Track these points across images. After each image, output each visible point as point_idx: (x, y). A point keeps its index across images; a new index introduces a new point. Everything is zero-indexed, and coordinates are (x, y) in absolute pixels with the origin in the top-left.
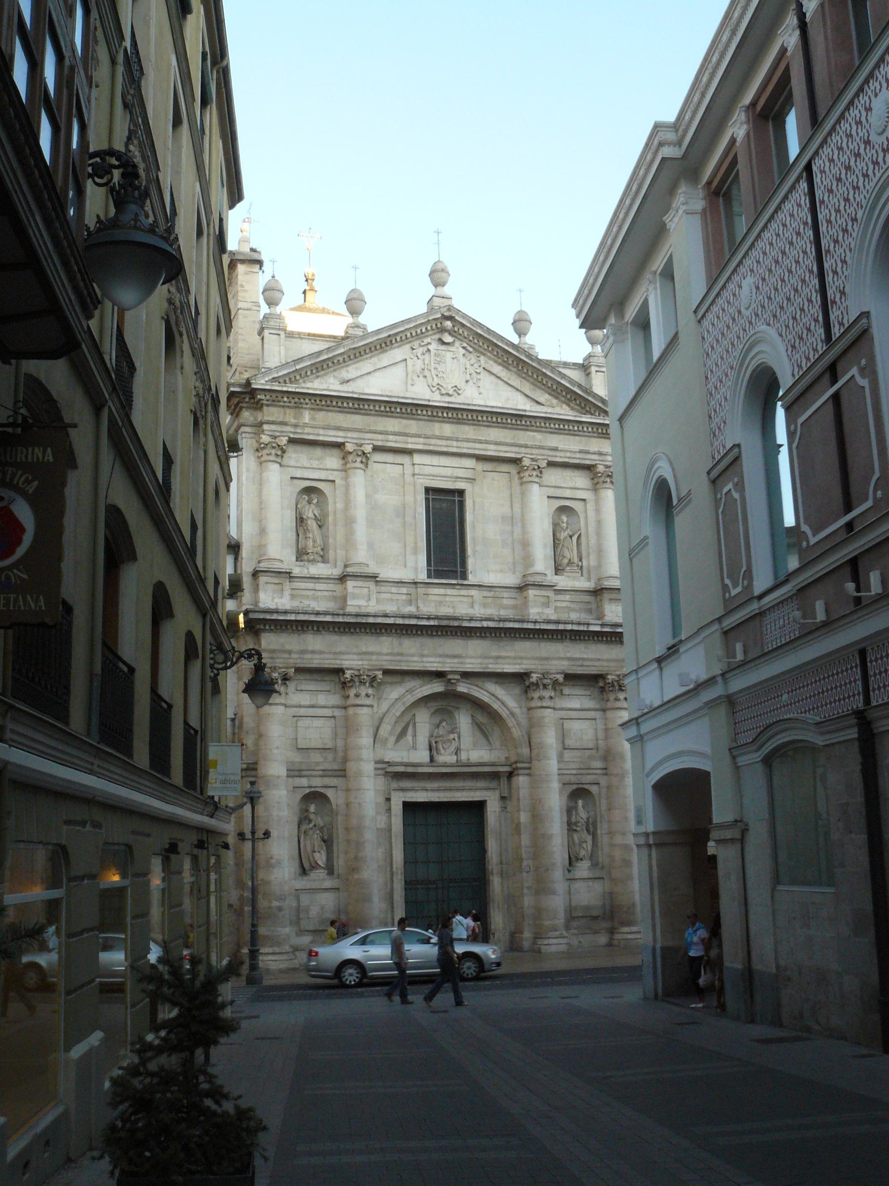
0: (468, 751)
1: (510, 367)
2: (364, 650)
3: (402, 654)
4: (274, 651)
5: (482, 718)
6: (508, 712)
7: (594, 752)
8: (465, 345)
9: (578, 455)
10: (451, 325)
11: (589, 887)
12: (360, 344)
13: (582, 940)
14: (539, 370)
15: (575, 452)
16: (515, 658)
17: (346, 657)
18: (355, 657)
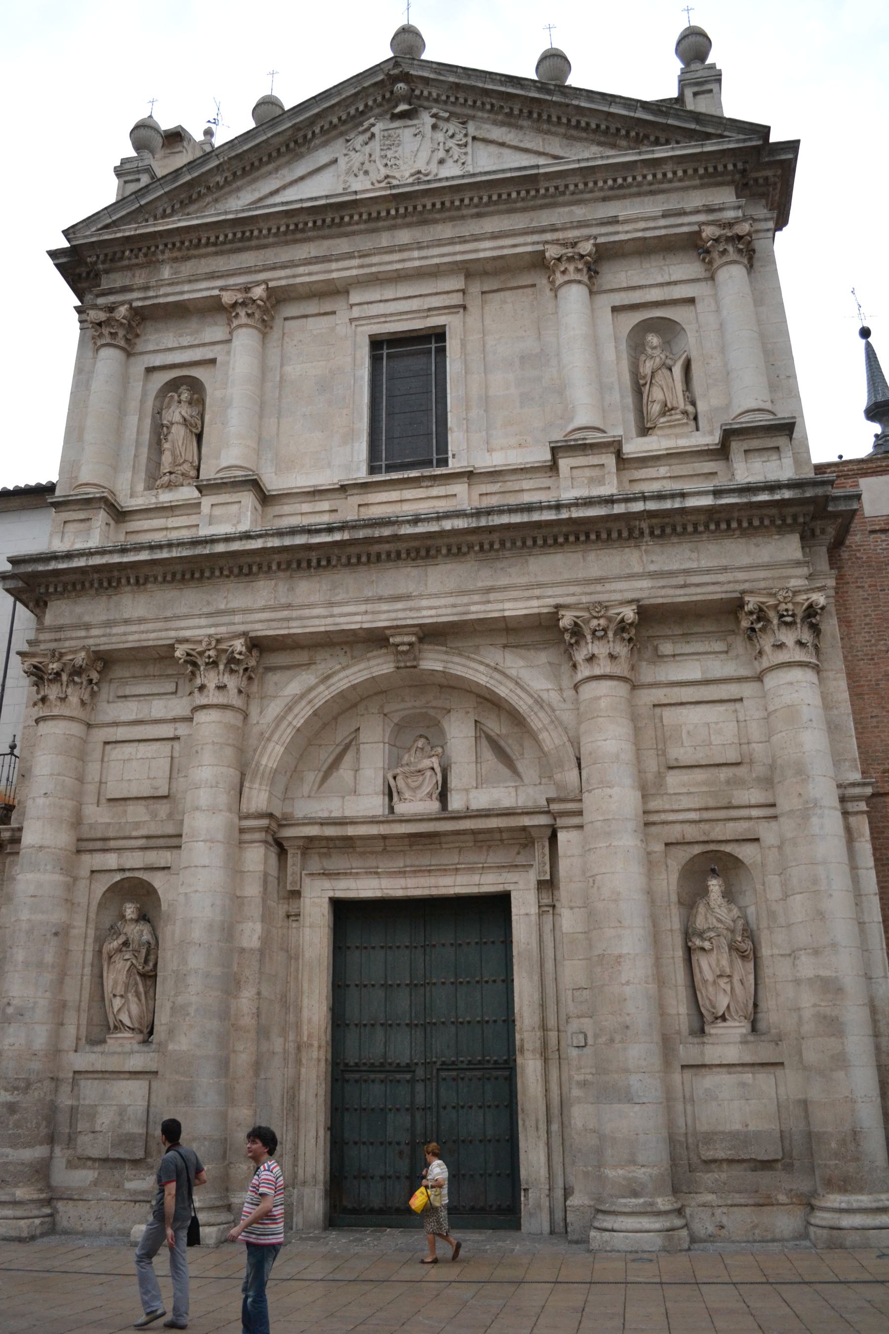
0: (467, 791)
1: (520, 122)
2: (222, 607)
3: (289, 606)
4: (60, 628)
5: (495, 726)
6: (530, 701)
7: (741, 771)
8: (434, 111)
9: (662, 222)
10: (406, 87)
11: (744, 1085)
12: (245, 148)
13: (725, 1220)
14: (568, 105)
15: (654, 218)
16: (529, 587)
17: (183, 624)
18: (203, 621)
